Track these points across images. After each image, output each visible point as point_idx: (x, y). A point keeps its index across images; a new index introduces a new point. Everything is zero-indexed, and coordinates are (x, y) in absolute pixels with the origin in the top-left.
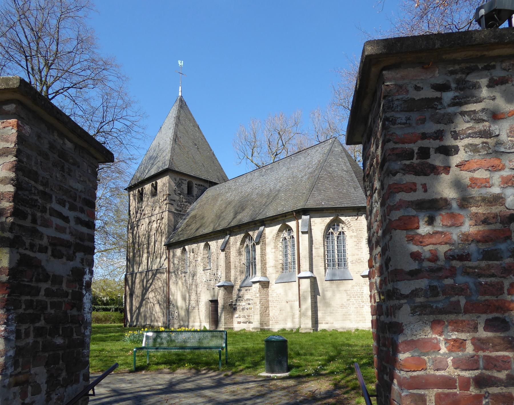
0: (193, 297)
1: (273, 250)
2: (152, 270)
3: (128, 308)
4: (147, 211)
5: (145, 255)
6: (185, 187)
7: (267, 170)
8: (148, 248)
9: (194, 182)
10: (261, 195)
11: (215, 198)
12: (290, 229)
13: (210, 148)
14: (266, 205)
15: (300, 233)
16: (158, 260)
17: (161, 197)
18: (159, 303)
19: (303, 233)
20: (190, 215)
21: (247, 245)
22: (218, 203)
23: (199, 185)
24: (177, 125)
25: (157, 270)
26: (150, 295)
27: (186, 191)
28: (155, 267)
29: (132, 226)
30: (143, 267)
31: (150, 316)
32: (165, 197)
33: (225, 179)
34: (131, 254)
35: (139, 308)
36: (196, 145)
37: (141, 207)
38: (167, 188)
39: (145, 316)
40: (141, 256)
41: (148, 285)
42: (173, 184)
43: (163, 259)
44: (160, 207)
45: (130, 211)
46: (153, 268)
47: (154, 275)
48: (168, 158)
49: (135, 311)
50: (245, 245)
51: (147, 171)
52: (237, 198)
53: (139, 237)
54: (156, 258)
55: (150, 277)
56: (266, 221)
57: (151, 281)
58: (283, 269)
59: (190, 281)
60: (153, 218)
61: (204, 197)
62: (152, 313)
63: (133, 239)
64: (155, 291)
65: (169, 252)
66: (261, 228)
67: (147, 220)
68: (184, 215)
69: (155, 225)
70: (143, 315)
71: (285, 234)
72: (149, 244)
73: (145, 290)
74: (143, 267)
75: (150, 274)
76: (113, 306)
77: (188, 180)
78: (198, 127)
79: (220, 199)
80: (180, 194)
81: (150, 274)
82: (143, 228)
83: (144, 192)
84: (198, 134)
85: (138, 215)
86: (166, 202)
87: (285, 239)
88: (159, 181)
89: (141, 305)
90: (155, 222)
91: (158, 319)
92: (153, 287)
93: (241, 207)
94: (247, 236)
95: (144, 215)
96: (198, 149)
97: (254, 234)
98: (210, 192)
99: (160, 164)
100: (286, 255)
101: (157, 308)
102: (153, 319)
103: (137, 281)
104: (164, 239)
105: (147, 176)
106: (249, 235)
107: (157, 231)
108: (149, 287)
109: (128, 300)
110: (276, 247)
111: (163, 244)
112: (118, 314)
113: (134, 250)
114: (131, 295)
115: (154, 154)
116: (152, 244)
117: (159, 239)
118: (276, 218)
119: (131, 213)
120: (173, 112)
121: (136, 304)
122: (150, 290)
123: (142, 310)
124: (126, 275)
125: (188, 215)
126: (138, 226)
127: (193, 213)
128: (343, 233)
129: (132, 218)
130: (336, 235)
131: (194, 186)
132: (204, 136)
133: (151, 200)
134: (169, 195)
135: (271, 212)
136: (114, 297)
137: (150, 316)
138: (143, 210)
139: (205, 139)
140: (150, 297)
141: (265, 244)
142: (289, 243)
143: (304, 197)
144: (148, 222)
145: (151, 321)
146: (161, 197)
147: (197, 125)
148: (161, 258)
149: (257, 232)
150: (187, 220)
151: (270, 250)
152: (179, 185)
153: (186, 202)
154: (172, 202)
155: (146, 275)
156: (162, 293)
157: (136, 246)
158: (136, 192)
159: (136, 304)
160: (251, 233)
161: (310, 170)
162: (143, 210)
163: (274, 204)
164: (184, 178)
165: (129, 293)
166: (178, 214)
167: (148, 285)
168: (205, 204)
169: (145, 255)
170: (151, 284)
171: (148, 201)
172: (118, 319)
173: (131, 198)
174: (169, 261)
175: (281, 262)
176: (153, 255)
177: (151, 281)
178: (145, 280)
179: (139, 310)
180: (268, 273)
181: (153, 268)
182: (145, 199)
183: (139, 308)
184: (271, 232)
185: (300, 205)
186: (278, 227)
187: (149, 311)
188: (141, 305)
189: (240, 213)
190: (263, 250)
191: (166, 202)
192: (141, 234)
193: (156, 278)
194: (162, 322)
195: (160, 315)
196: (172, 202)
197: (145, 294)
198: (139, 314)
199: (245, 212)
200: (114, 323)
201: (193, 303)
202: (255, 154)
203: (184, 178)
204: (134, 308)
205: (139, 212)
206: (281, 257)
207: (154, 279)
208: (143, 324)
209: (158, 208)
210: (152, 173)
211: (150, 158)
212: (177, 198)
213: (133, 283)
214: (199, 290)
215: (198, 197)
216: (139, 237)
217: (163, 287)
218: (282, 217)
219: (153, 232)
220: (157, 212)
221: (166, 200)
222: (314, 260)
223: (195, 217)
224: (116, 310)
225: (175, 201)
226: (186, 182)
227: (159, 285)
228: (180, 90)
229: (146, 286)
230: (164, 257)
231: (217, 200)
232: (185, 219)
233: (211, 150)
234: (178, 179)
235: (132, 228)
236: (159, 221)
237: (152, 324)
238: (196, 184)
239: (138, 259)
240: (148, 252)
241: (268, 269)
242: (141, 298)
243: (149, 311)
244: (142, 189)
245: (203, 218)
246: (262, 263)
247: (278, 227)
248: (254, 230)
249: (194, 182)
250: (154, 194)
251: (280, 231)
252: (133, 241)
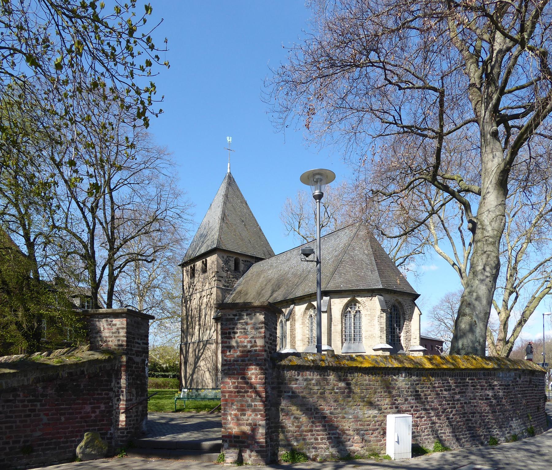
1: (301, 326)
2: (203, 341)
4: (199, 286)
5: (197, 327)
6: (232, 264)
8: (199, 320)
9: (241, 259)
10: (295, 275)
11: (259, 275)
13: (257, 223)
14: (297, 285)
16: (208, 331)
17: (210, 273)
20: (237, 291)
22: (261, 280)
23: (245, 261)
24: (225, 203)
25: (207, 341)
26: (202, 363)
27: (233, 268)
28: (205, 338)
29: (186, 300)
30: (195, 338)
31: (202, 382)
32: (214, 274)
33: (271, 254)
34: (185, 326)
35: (192, 375)
36: (243, 221)
37: (193, 283)
38: (216, 266)
39: (197, 382)
40: (193, 328)
41: (200, 355)
42: (221, 262)
43: (212, 331)
44: (210, 283)
45: (183, 286)
46: (204, 339)
47: (205, 345)
48: (216, 237)
49: (189, 378)
51: (198, 249)
52: (276, 276)
53: (192, 310)
54: (207, 330)
55: (201, 347)
57: (202, 351)
58: (309, 343)
60: (204, 293)
61: (249, 272)
62: (203, 380)
63: (187, 312)
65: (217, 324)
66: (292, 306)
67: (198, 295)
68: (231, 290)
69: (205, 300)
70: (195, 381)
71: (311, 312)
72: (200, 317)
74: (195, 338)
75: (201, 344)
76: (171, 373)
78: (246, 204)
79: (262, 276)
80: (227, 271)
81: (201, 344)
82: (194, 303)
83: (196, 268)
84: (245, 210)
85: (191, 290)
86: (214, 279)
87: (311, 316)
88: (208, 259)
90: (205, 297)
92: (203, 356)
93: (277, 286)
95: (196, 290)
96: (245, 225)
98: (256, 268)
99: (209, 243)
100: (312, 331)
101: (207, 375)
102: (204, 384)
103: (191, 350)
104: (213, 313)
105: (198, 254)
107: (207, 305)
109: (183, 368)
110: (303, 323)
111: (212, 317)
112: (176, 381)
113: (187, 322)
114: (186, 363)
115: (205, 232)
116: (203, 317)
117: (209, 313)
118: (304, 298)
119: (185, 287)
120: (222, 190)
121: (189, 371)
122: (201, 358)
123: (194, 377)
124: (181, 345)
125: (235, 290)
126: (190, 300)
127: (239, 289)
129: (185, 292)
130: (353, 313)
131: (241, 262)
132: (251, 212)
133: (202, 276)
134: (217, 272)
135: (299, 293)
136: (172, 365)
137: (202, 382)
138: (195, 286)
141: (295, 320)
142: (314, 320)
143: (327, 279)
144: (199, 297)
146: (210, 273)
148: (210, 330)
149: (288, 309)
150: (233, 295)
151: (298, 325)
152: (226, 262)
153: (233, 278)
154: (219, 278)
156: (211, 362)
157: (189, 318)
158: (189, 268)
159: (189, 371)
161: (336, 253)
162: (195, 286)
163: (303, 285)
164: (232, 256)
166: (225, 290)
167: (200, 355)
168: (250, 280)
169: (197, 327)
170: (202, 353)
171: (199, 277)
172: (176, 385)
173: (185, 274)
174: (217, 333)
175: (308, 336)
176: (204, 327)
177: (202, 351)
179: (192, 377)
180: (296, 345)
181: (204, 339)
182: (196, 275)
183: (192, 375)
184: (300, 310)
186: (305, 305)
187: (200, 378)
189: (276, 291)
190: (292, 326)
191: (214, 279)
192: (193, 308)
195: (210, 381)
196: (220, 279)
197: (198, 362)
198: (192, 380)
199: (280, 290)
200: (172, 388)
202: (303, 224)
203: (232, 256)
204: (188, 375)
205: (192, 287)
206: (307, 332)
207: (204, 349)
209: (207, 284)
210: (203, 252)
211: (201, 236)
212: (225, 274)
213: (187, 352)
215: (244, 272)
216: (192, 310)
217: (213, 356)
218: (308, 297)
219: (203, 307)
220: (206, 287)
221: (214, 276)
222: (332, 335)
223: (240, 292)
224: (174, 376)
225: (222, 277)
228: (229, 167)
230: (213, 329)
231: (260, 277)
232: (232, 294)
234: (225, 257)
235: (186, 302)
236: (208, 296)
239: (191, 330)
240: (199, 325)
241: (296, 342)
243: (200, 378)
244: (194, 266)
245: (247, 294)
246: (291, 337)
247: (305, 305)
248: (286, 307)
249: (241, 259)
250: (204, 270)
251: (307, 309)
252: (186, 314)
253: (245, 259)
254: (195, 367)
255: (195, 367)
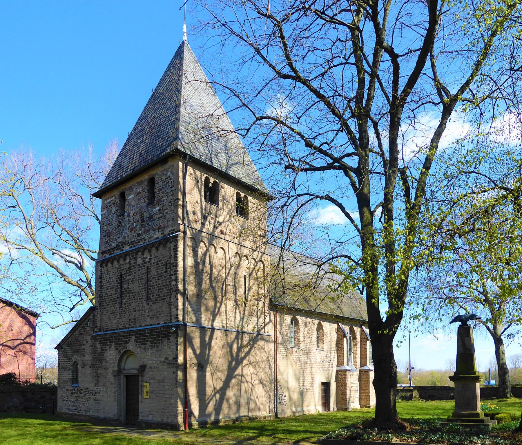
0: (308, 378)
3: (192, 391)
18: (262, 383)
31: (248, 403)
35: (223, 391)
41: (242, 355)
55: (245, 343)
57: (247, 349)
59: (303, 359)
62: (249, 399)
64: (255, 364)
73: (235, 362)
75: (246, 338)
89: (226, 385)
91: (262, 407)
92: (250, 358)
101: (260, 391)
108: (245, 357)
121: (213, 381)
122: (245, 362)
123: (230, 393)
140: (244, 373)
145: (249, 410)
155: (237, 337)
159: (213, 381)
165: (195, 361)
170: (248, 354)
178: (235, 346)
183: (223, 391)
188: (226, 385)
193: (255, 346)
194: (268, 410)
197: (236, 368)
201: (307, 385)
204: (209, 391)
208: (233, 416)
213: (206, 346)
214: (313, 370)
227: (261, 357)
229: (238, 355)
237: (250, 415)
242: (226, 373)
254: (230, 376)
255: (230, 376)
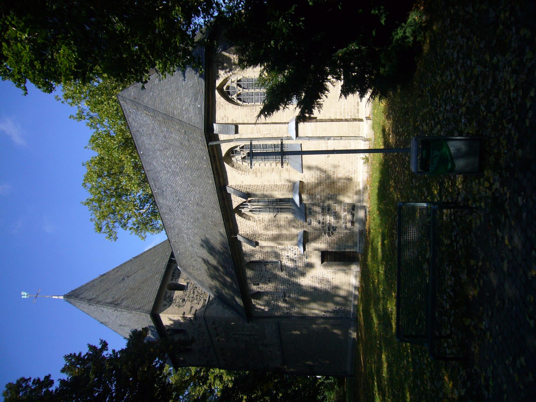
7: (156, 186)
9: (169, 282)
12: (232, 152)
15: (237, 136)
19: (237, 132)
21: (250, 211)
23: (173, 276)
36: (124, 279)
50: (250, 214)
56: (220, 183)
66: (229, 190)
77: (166, 289)
78: (104, 275)
94: (238, 210)
96: (128, 277)
97: (236, 201)
106: (238, 207)
128: (240, 81)
132: (114, 269)
139: (117, 267)
147: (100, 277)
153: (194, 293)
160: (234, 206)
185: (200, 135)
186: (227, 167)
206: (268, 164)
218: (215, 160)
225: (192, 307)
226: (169, 292)
233: (131, 260)
234: (165, 302)
238: (172, 280)
249: (169, 282)
253: (170, 277)
